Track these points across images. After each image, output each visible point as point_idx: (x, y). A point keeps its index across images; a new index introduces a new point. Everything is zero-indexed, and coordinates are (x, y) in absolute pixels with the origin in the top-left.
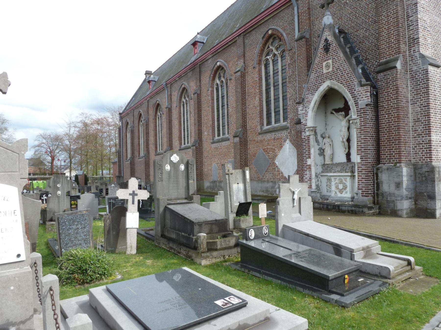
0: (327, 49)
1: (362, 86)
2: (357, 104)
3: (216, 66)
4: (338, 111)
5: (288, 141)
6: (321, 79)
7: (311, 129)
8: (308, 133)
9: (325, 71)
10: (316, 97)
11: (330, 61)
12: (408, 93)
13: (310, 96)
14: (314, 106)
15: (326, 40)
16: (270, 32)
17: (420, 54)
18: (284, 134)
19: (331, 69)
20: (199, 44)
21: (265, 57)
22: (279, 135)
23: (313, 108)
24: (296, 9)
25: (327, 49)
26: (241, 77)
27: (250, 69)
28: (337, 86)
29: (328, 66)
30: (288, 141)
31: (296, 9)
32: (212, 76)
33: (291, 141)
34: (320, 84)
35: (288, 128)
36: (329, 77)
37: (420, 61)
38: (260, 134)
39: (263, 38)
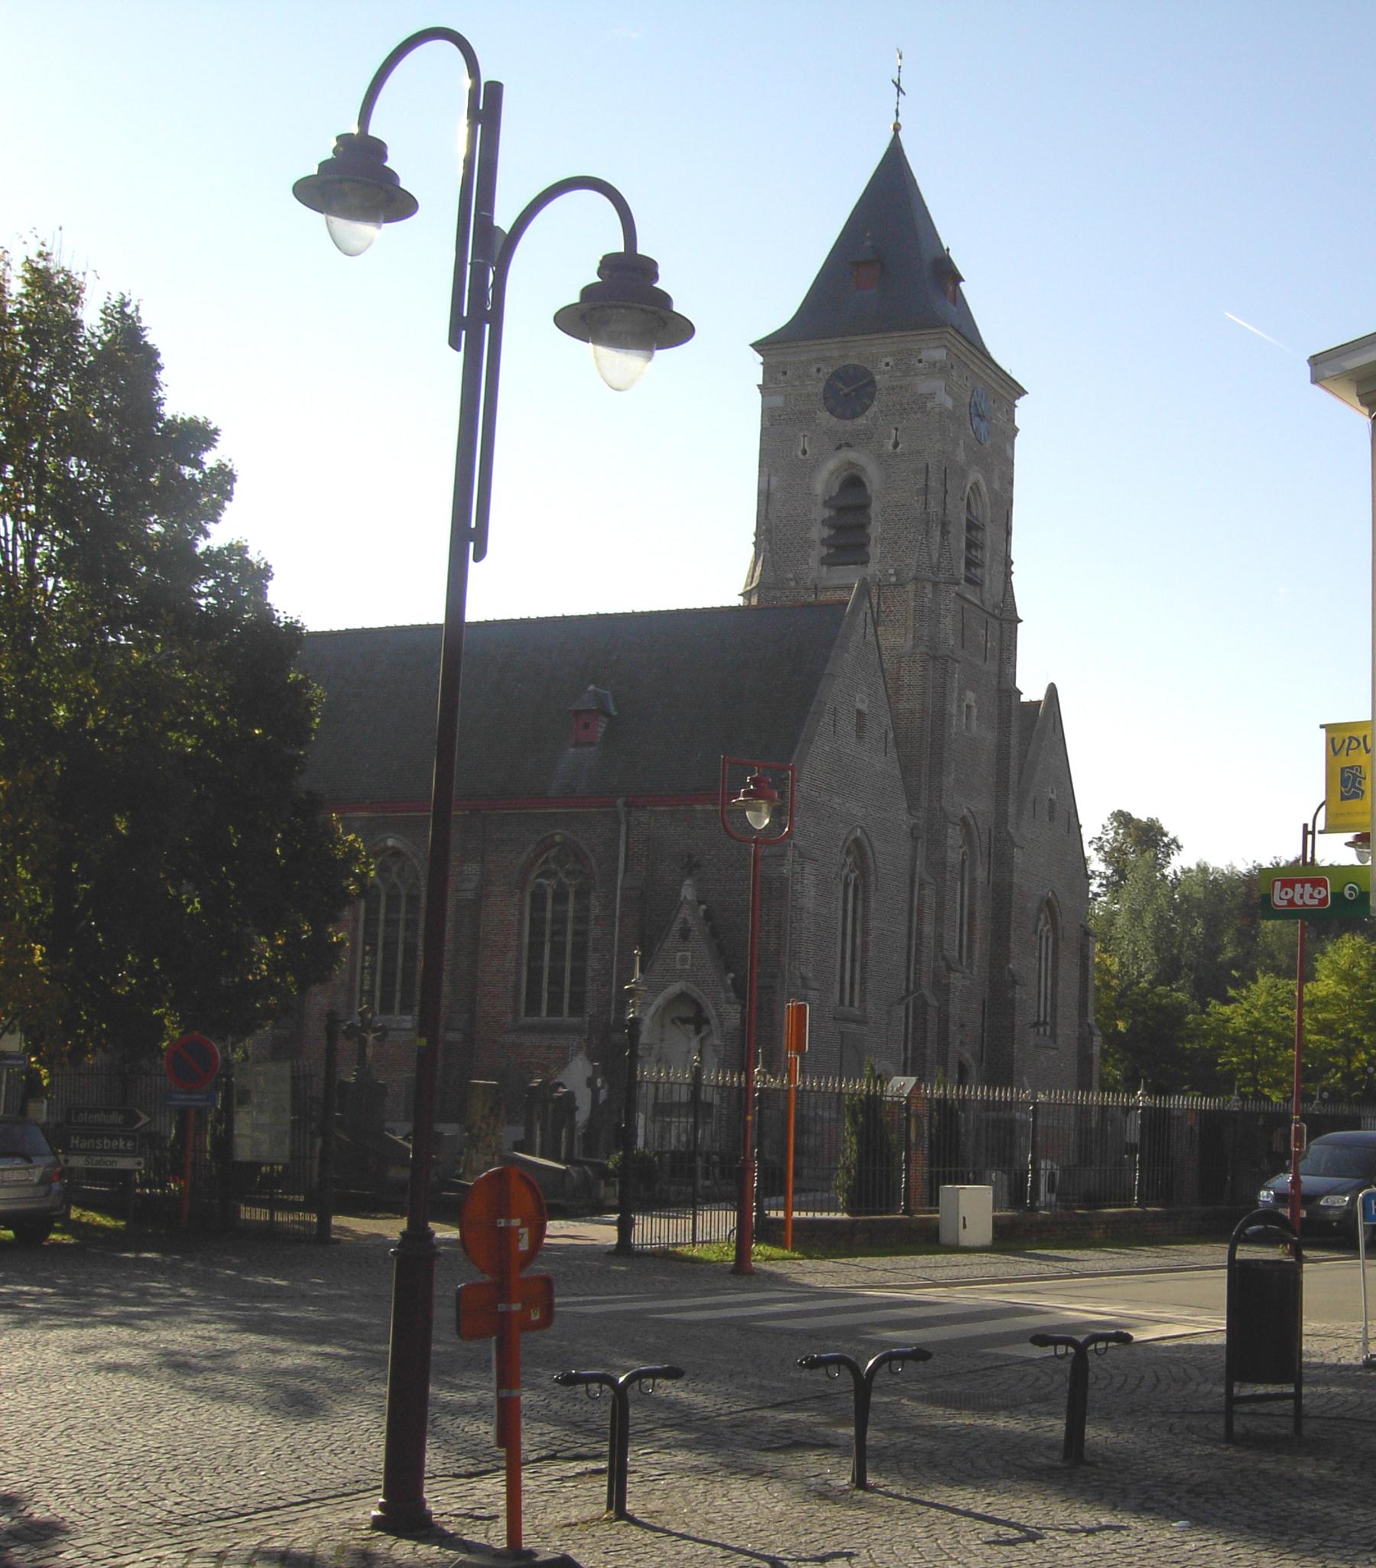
0: (685, 934)
2: (722, 1025)
4: (685, 1021)
9: (678, 966)
10: (659, 1001)
15: (685, 921)
16: (558, 838)
17: (801, 973)
19: (687, 967)
21: (537, 878)
24: (623, 828)
25: (685, 934)
29: (683, 960)
31: (623, 828)
37: (799, 982)
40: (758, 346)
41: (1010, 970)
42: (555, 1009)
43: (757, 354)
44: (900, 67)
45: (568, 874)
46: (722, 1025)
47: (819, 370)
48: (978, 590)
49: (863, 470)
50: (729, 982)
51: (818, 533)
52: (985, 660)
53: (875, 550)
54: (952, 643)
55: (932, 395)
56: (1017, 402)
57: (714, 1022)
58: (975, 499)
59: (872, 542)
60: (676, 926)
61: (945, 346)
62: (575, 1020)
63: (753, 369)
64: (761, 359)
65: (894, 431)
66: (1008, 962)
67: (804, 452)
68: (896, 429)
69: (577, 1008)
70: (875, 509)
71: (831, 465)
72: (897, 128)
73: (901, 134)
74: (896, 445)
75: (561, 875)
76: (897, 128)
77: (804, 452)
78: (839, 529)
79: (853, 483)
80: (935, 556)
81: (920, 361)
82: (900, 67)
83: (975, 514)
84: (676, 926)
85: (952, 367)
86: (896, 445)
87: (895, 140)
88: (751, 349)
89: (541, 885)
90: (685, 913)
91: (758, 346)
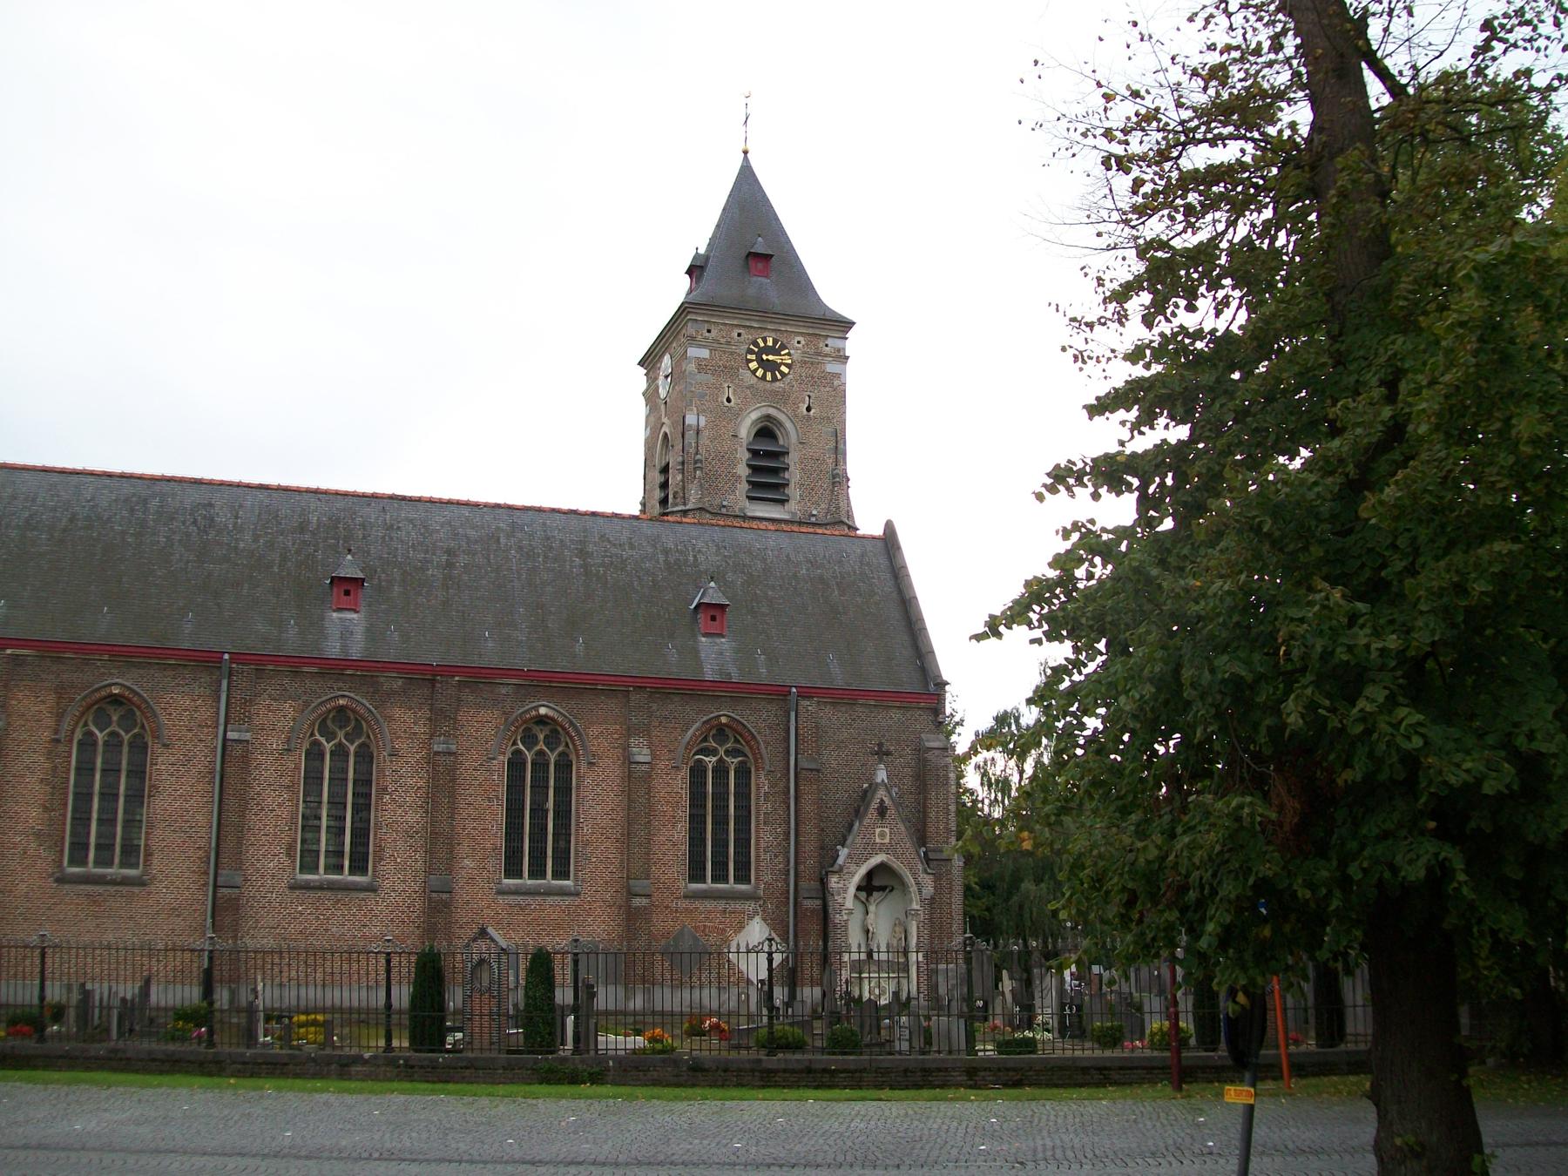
0: (882, 811)
2: (920, 892)
3: (534, 713)
5: (757, 919)
6: (874, 849)
8: (845, 917)
10: (863, 870)
11: (887, 830)
13: (853, 867)
15: (882, 800)
16: (724, 720)
18: (750, 906)
19: (887, 840)
22: (738, 906)
24: (793, 714)
25: (882, 811)
28: (896, 864)
29: (882, 835)
30: (757, 919)
31: (793, 714)
33: (764, 920)
34: (870, 855)
35: (760, 898)
36: (882, 849)
38: (686, 897)
42: (720, 876)
45: (727, 752)
46: (920, 892)
47: (739, 335)
49: (780, 424)
53: (794, 492)
57: (913, 888)
59: (792, 485)
60: (874, 805)
62: (743, 887)
67: (729, 400)
69: (743, 875)
70: (793, 459)
71: (754, 416)
72: (746, 152)
74: (809, 409)
75: (722, 752)
76: (746, 152)
77: (729, 400)
78: (755, 469)
79: (766, 431)
84: (874, 805)
86: (809, 409)
87: (746, 159)
89: (700, 761)
90: (881, 793)
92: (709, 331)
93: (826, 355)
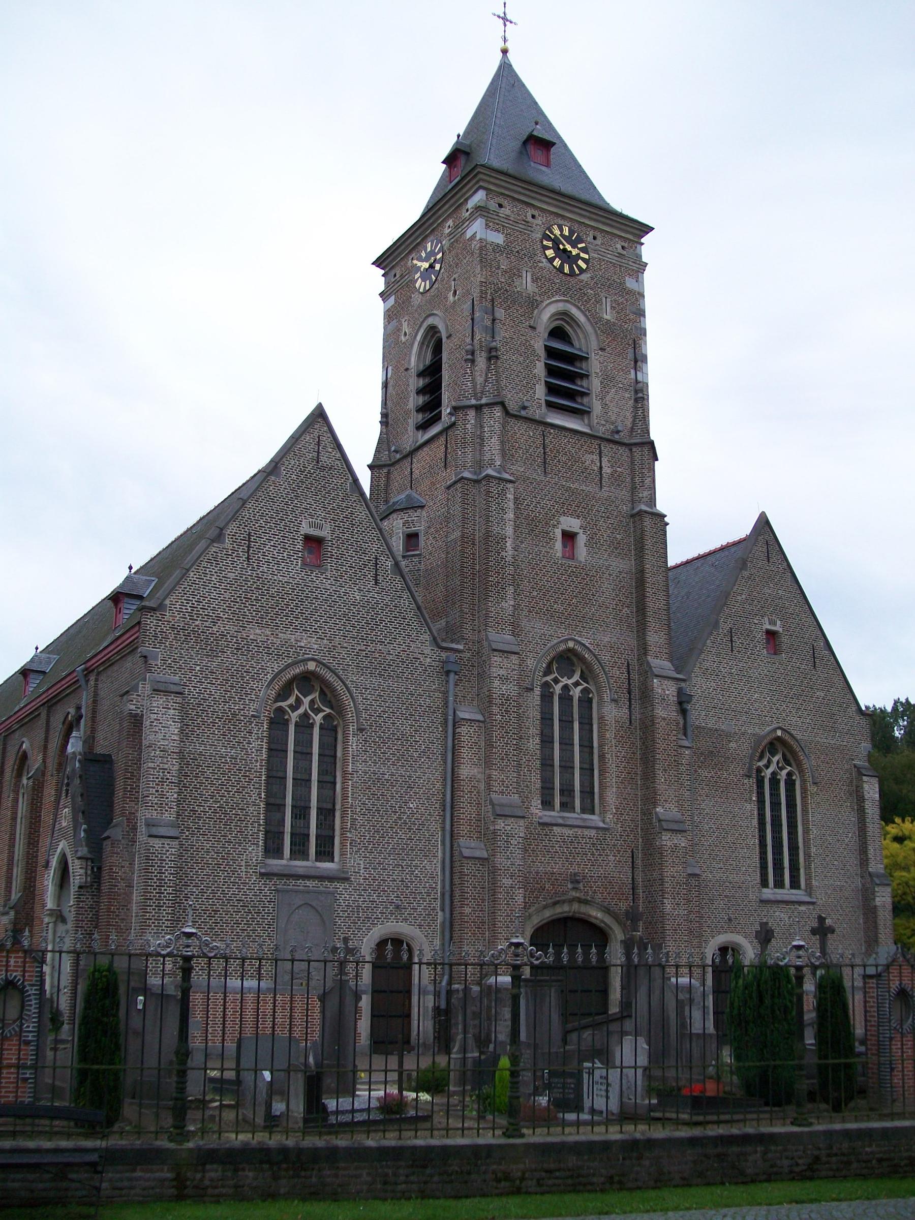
1: (79, 858)
7: (48, 912)
12: (133, 874)
14: (54, 876)
20: (32, 676)
23: (53, 880)
26: (34, 789)
27: (48, 777)
32: (16, 767)
39: (64, 723)
40: (379, 263)
41: (656, 813)
43: (378, 269)
44: (505, 4)
48: (586, 421)
50: (82, 834)
51: (414, 401)
52: (601, 488)
54: (499, 463)
55: (474, 236)
56: (643, 240)
58: (575, 331)
61: (481, 187)
63: (377, 279)
64: (383, 272)
65: (453, 282)
66: (655, 804)
67: (405, 334)
68: (454, 280)
71: (419, 338)
72: (505, 52)
73: (512, 57)
76: (505, 52)
77: (405, 334)
80: (480, 380)
81: (467, 210)
82: (505, 4)
83: (578, 347)
85: (500, 206)
88: (374, 266)
91: (379, 263)
92: (395, 275)
93: (465, 220)
